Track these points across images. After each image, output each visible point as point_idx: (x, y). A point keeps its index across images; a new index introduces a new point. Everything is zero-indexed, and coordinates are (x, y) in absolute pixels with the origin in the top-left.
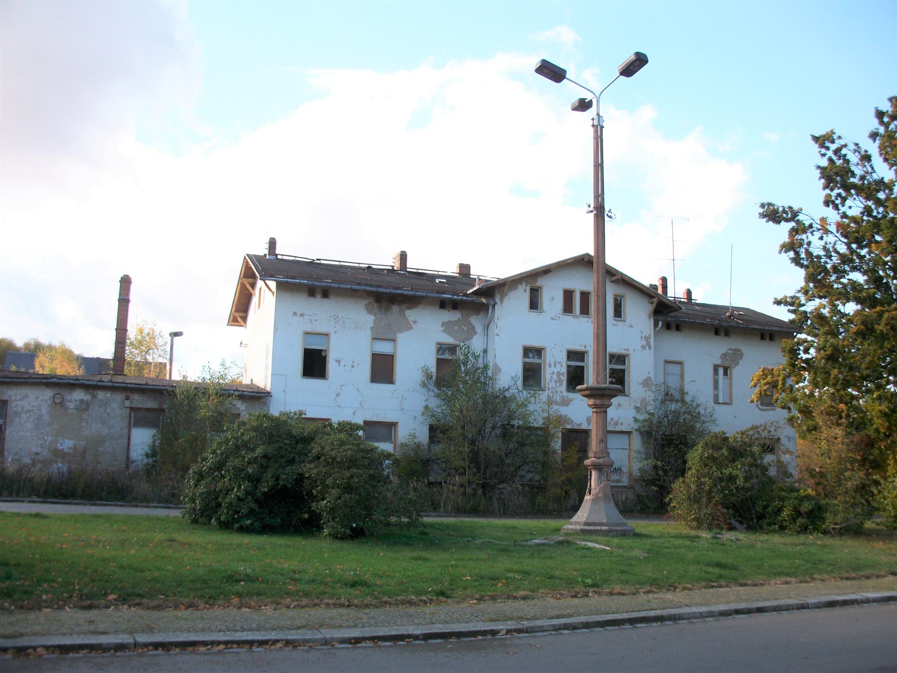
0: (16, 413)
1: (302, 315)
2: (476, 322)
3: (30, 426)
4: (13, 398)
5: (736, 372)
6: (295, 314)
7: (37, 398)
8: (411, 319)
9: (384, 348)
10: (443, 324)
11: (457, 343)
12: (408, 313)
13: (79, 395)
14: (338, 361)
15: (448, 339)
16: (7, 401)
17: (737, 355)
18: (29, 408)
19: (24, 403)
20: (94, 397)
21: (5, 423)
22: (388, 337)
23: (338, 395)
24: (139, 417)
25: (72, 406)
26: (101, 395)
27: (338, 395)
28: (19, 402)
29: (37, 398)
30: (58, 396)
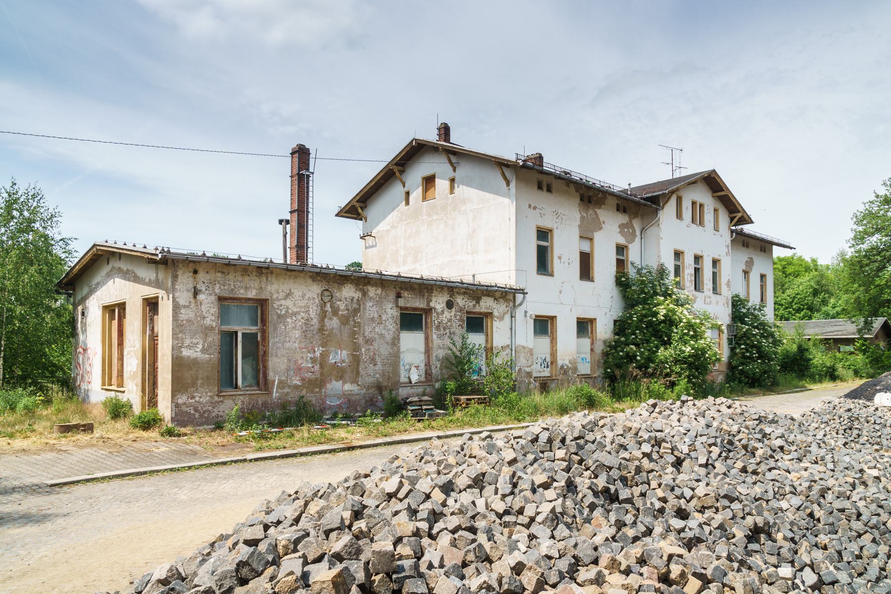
0: (279, 316)
1: (535, 208)
2: (637, 225)
3: (297, 334)
4: (275, 296)
5: (751, 275)
6: (530, 206)
7: (303, 296)
8: (601, 219)
9: (586, 248)
10: (620, 227)
11: (626, 244)
12: (599, 211)
13: (349, 292)
14: (560, 258)
15: (622, 241)
16: (266, 300)
17: (750, 263)
18: (295, 310)
19: (288, 303)
20: (365, 294)
21: (264, 332)
22: (590, 236)
23: (560, 292)
24: (411, 320)
25: (342, 306)
26: (372, 291)
27: (560, 292)
28: (283, 302)
29: (303, 296)
30: (326, 293)
